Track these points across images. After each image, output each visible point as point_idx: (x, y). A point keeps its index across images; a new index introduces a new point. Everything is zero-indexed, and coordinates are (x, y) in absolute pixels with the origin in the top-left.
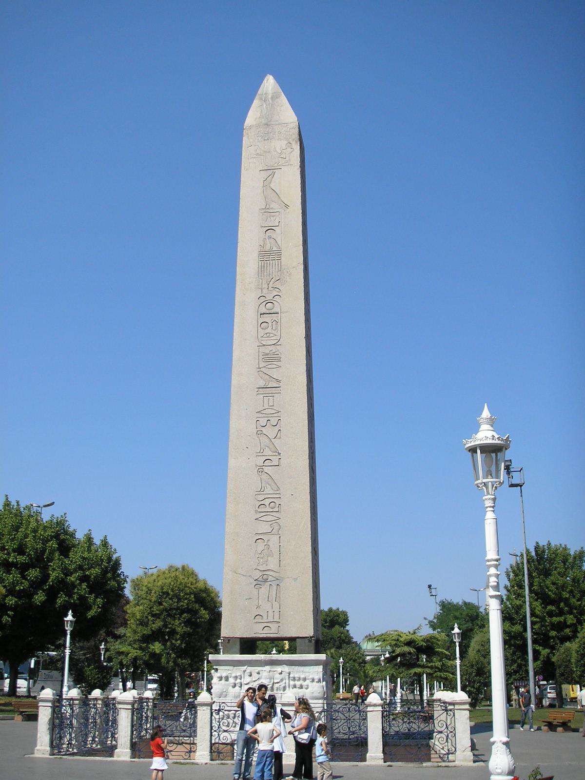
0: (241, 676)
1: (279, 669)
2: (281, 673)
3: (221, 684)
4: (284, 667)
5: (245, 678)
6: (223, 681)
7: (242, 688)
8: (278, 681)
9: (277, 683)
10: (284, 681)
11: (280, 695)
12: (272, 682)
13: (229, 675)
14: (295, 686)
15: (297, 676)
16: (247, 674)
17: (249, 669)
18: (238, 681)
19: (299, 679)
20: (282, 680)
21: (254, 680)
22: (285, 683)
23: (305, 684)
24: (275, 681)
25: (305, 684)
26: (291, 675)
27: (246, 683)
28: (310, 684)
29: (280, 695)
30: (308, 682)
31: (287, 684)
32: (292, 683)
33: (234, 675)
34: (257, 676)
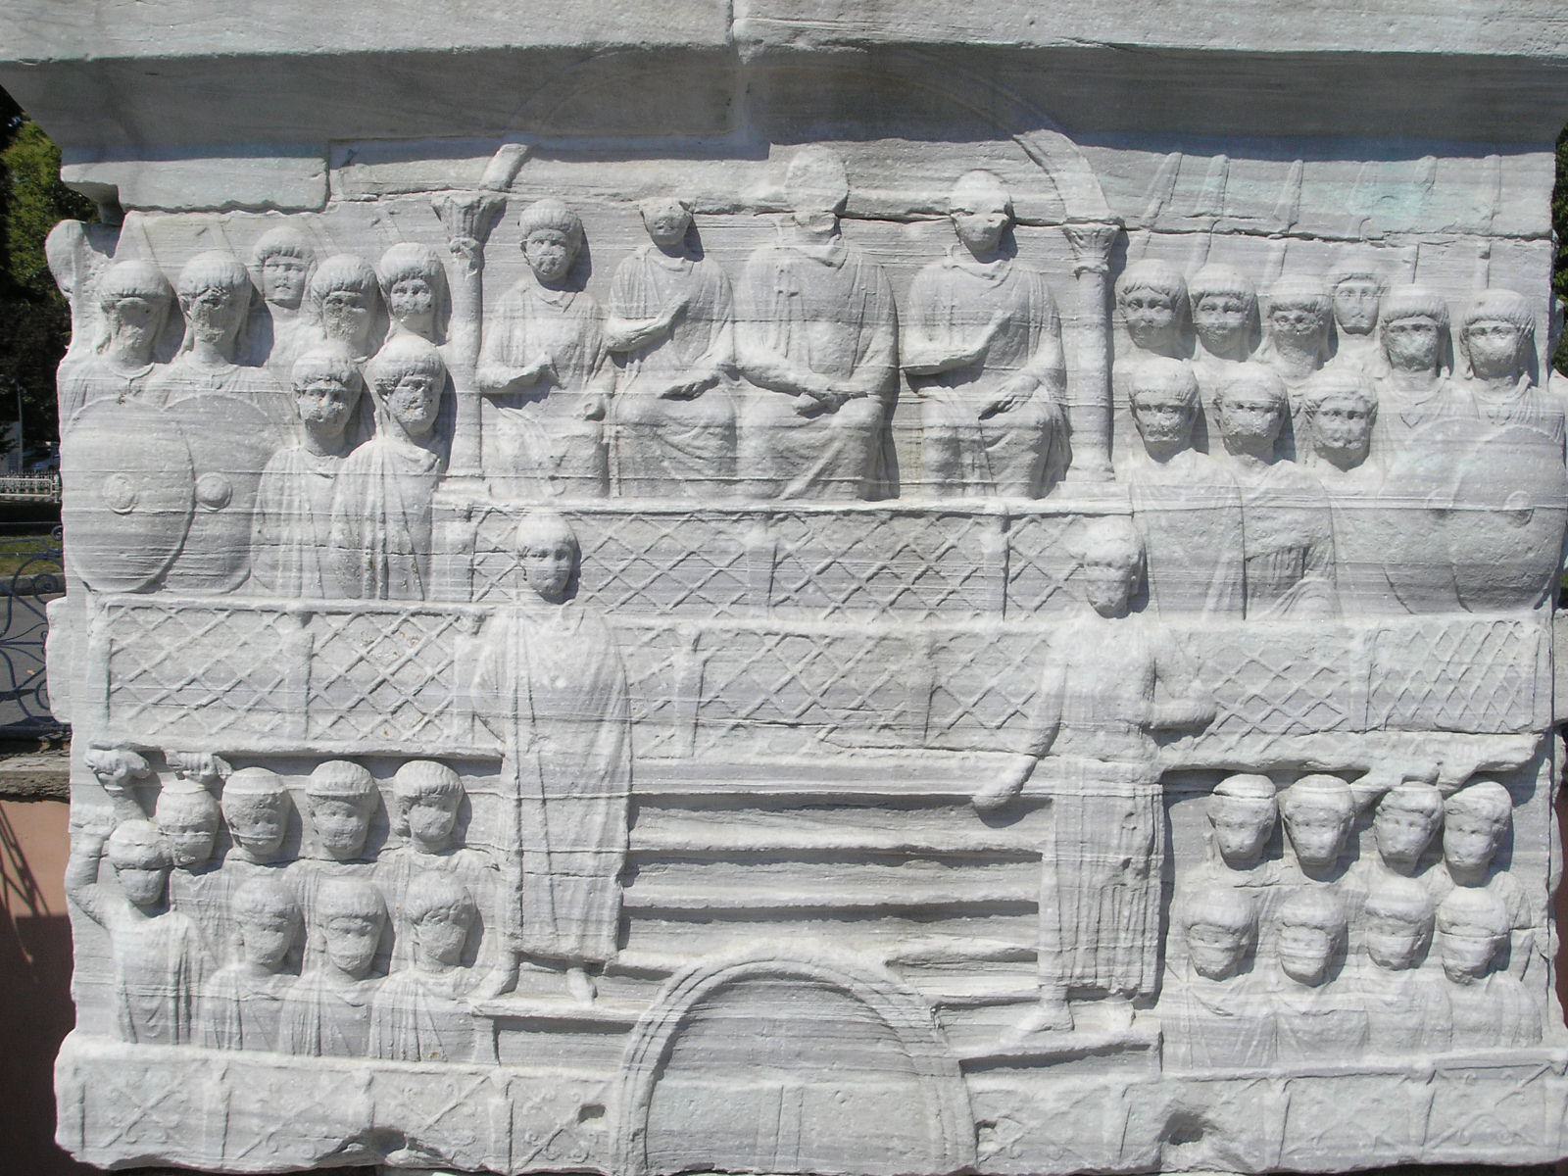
0: (436, 283)
1: (974, 183)
2: (998, 244)
3: (164, 395)
5: (498, 304)
6: (192, 366)
7: (461, 445)
8: (968, 343)
10: (1043, 358)
11: (991, 540)
12: (871, 371)
13: (273, 280)
14: (1191, 425)
15: (1214, 276)
17: (551, 190)
18: (403, 348)
19: (1247, 329)
20: (1015, 335)
21: (619, 329)
22: (1060, 378)
26: (1144, 273)
27: (497, 374)
28: (1394, 393)
29: (991, 540)
30: (1355, 368)
31: (1084, 396)
32: (1155, 375)
33: (335, 269)
34: (666, 283)
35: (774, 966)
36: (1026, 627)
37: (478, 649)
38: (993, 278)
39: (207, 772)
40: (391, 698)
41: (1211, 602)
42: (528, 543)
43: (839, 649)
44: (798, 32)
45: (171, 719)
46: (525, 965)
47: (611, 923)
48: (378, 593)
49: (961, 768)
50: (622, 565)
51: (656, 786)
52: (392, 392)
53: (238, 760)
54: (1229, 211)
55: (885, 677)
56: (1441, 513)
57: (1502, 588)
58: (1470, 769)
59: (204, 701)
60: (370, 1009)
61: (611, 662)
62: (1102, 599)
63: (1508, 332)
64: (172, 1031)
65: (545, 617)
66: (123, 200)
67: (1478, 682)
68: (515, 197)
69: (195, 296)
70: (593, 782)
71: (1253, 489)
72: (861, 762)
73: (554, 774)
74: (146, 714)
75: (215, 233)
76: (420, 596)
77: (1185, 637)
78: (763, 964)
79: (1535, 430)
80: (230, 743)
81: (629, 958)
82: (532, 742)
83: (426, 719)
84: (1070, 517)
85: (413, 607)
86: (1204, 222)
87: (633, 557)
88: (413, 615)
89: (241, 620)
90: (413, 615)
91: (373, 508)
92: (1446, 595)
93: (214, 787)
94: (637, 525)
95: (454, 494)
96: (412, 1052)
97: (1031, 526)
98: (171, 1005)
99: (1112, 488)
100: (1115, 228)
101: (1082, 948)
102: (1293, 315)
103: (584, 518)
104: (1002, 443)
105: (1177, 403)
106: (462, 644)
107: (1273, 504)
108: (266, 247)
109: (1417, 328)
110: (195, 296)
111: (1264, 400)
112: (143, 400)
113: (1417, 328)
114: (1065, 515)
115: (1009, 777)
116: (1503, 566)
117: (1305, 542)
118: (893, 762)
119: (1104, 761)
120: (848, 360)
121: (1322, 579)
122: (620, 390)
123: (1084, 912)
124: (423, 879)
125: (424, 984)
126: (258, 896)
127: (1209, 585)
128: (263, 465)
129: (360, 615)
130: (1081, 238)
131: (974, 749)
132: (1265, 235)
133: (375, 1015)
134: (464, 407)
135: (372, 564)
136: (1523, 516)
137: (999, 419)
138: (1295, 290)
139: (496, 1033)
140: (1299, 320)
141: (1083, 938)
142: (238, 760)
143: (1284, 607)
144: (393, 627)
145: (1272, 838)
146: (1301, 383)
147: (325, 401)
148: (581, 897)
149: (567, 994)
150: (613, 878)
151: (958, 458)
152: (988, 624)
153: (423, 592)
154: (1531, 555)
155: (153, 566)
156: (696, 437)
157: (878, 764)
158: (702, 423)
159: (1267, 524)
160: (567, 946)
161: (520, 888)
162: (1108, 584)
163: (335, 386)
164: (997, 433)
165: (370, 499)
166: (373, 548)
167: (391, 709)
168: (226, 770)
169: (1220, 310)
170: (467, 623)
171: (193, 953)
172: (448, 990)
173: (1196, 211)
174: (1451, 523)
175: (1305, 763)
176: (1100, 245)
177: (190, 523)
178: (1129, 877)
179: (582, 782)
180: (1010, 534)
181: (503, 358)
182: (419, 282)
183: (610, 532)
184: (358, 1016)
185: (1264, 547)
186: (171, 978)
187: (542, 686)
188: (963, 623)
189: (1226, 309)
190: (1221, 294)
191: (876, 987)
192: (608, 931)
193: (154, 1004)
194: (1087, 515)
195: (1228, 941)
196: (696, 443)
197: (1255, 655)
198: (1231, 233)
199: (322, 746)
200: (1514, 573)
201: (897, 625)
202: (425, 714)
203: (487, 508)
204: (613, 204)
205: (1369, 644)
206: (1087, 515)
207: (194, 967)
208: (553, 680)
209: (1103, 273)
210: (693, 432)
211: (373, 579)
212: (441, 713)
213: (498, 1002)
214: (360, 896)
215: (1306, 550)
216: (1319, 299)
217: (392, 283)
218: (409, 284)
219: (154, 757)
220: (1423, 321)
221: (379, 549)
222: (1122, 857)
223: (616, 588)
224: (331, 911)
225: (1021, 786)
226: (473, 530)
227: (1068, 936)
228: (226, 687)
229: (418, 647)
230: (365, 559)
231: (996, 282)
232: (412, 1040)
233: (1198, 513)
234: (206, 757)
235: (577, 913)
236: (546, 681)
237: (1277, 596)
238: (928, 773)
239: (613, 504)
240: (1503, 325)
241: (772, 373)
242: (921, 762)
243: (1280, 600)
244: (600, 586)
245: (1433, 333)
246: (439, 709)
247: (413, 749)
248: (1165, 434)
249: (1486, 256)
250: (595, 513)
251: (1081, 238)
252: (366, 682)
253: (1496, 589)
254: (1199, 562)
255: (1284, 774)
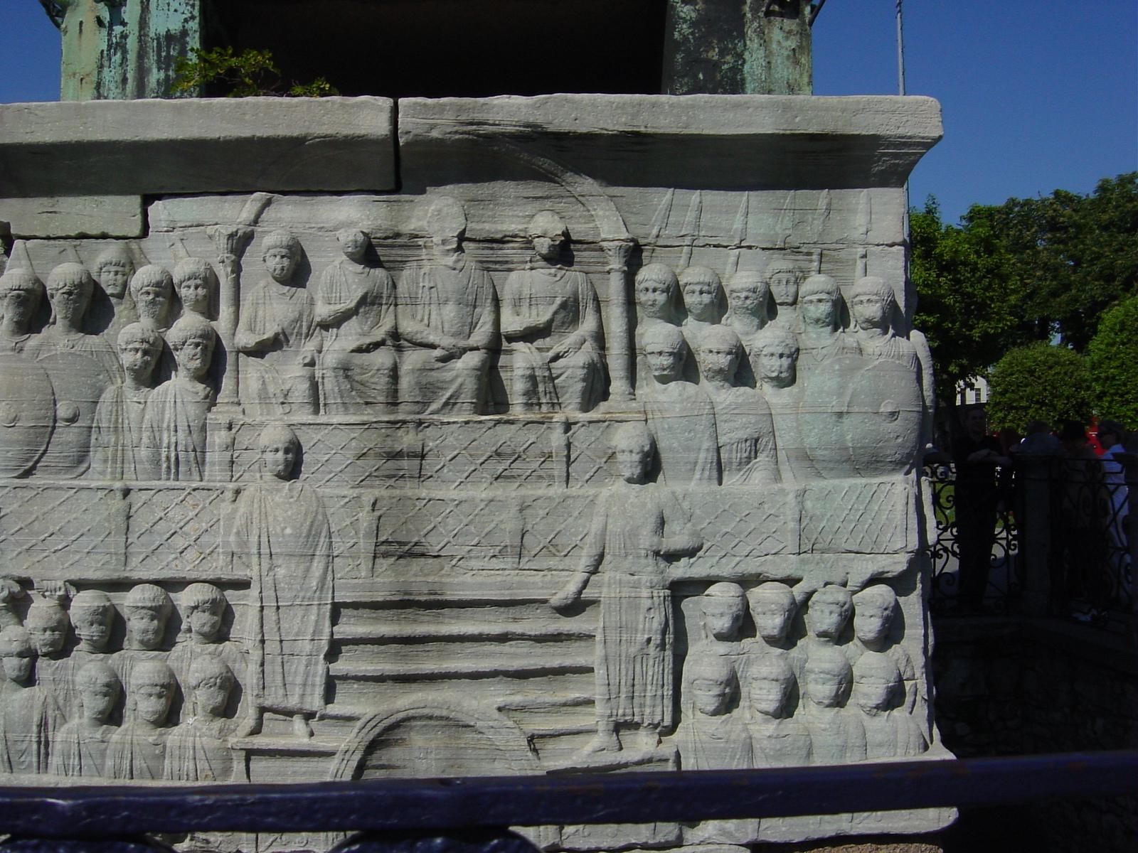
0: (210, 283)
2: (563, 253)
4: (579, 200)
5: (247, 298)
6: (57, 336)
7: (227, 382)
8: (541, 316)
9: (530, 335)
10: (588, 324)
12: (481, 335)
13: (108, 283)
14: (684, 365)
16: (264, 259)
18: (188, 323)
20: (570, 311)
21: (323, 311)
22: (600, 338)
23: (766, 343)
24: (511, 323)
25: (766, 343)
27: (246, 338)
32: (656, 335)
35: (426, 711)
36: (581, 492)
37: (235, 511)
38: (555, 276)
39: (59, 593)
40: (180, 542)
41: (697, 476)
42: (267, 444)
43: (464, 507)
44: (432, 127)
45: (37, 559)
46: (266, 715)
47: (321, 685)
48: (172, 476)
49: (542, 582)
50: (327, 457)
51: (349, 597)
52: (181, 349)
53: (81, 585)
54: (703, 233)
55: (493, 525)
56: (840, 415)
57: (882, 462)
58: (867, 576)
59: (60, 547)
60: (165, 747)
61: (320, 517)
62: (627, 474)
63: (877, 302)
64: (35, 764)
65: (278, 490)
66: (12, 231)
67: (870, 521)
68: (260, 229)
69: (57, 290)
70: (309, 594)
71: (721, 403)
72: (479, 579)
73: (284, 589)
74: (21, 556)
75: (71, 252)
76: (198, 479)
77: (681, 497)
78: (419, 710)
79: (897, 362)
80: (75, 575)
81: (333, 709)
82: (270, 569)
83: (202, 556)
84: (607, 423)
85: (194, 485)
86: (687, 241)
87: (334, 452)
88: (194, 490)
89: (84, 494)
90: (194, 490)
91: (169, 422)
92: (846, 466)
93: (65, 602)
94: (337, 432)
95: (220, 415)
96: (192, 775)
97: (583, 429)
98: (35, 746)
99: (634, 404)
100: (631, 244)
101: (623, 696)
102: (743, 295)
103: (303, 427)
104: (562, 378)
105: (671, 350)
106: (225, 508)
107: (735, 412)
108: (103, 260)
109: (820, 301)
110: (57, 290)
111: (725, 347)
112: (24, 355)
113: (820, 301)
114: (604, 421)
115: (571, 588)
116: (881, 448)
117: (756, 436)
118: (499, 579)
119: (632, 575)
120: (467, 329)
121: (767, 459)
122: (325, 349)
123: (623, 672)
124: (200, 660)
125: (199, 730)
126: (93, 673)
127: (696, 463)
128: (99, 397)
129: (160, 490)
130: (610, 250)
131: (550, 570)
132: (726, 247)
133: (168, 750)
134: (230, 359)
135: (168, 458)
136: (894, 415)
137: (561, 362)
138: (744, 280)
139: (248, 761)
140: (747, 298)
141: (623, 689)
142: (81, 585)
143: (745, 477)
144: (181, 498)
145: (743, 626)
146: (751, 337)
147: (139, 354)
148: (302, 668)
149: (291, 734)
150: (322, 656)
151: (542, 388)
152: (558, 490)
153: (201, 476)
154: (900, 440)
155: (27, 460)
156: (372, 376)
157: (489, 580)
158: (376, 368)
159: (732, 424)
160: (293, 702)
161: (262, 664)
162: (629, 464)
163: (145, 346)
164: (559, 372)
165: (167, 416)
166: (169, 448)
167: (180, 550)
168: (73, 591)
169: (697, 293)
170: (229, 495)
171: (50, 712)
172: (215, 732)
173: (682, 234)
174: (846, 421)
175: (761, 574)
176: (622, 253)
177: (52, 433)
178: (652, 649)
179: (301, 594)
180: (568, 434)
181: (251, 329)
182: (199, 282)
183: (319, 437)
184: (157, 752)
185: (731, 439)
186: (35, 729)
187: (276, 534)
188: (541, 490)
189: (701, 292)
190: (698, 283)
191: (491, 723)
192: (319, 690)
193: (24, 746)
194: (617, 421)
195: (716, 691)
196: (372, 380)
197: (727, 507)
198: (704, 246)
199: (135, 575)
200: (888, 452)
201: (499, 491)
202: (201, 553)
203: (242, 422)
204: (320, 233)
205: (799, 499)
206: (617, 421)
207: (50, 721)
208: (283, 529)
209: (624, 272)
210: (370, 374)
211: (169, 467)
212: (212, 552)
213: (247, 740)
214: (159, 672)
215: (757, 440)
216: (759, 284)
217: (181, 282)
218: (192, 283)
219: (26, 583)
220: (824, 296)
221: (173, 448)
222: (646, 636)
223: (323, 471)
224: (140, 682)
225: (580, 592)
226: (232, 436)
227: (614, 689)
228: (73, 538)
229: (197, 511)
230: (164, 455)
231: (558, 278)
232: (192, 766)
233: (687, 418)
234: (60, 583)
235: (299, 680)
236: (278, 529)
237: (739, 470)
238: (521, 585)
239: (322, 418)
240: (874, 298)
241: (419, 336)
242: (517, 579)
243: (742, 473)
244: (313, 470)
245: (830, 304)
246: (211, 549)
247: (194, 575)
248: (664, 370)
249: (865, 256)
250: (310, 424)
251: (610, 250)
252: (164, 534)
253: (878, 462)
254: (688, 449)
255: (747, 582)
